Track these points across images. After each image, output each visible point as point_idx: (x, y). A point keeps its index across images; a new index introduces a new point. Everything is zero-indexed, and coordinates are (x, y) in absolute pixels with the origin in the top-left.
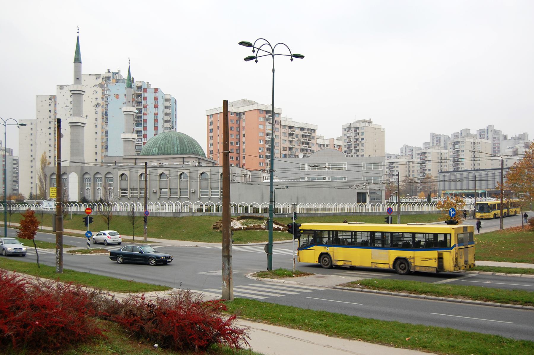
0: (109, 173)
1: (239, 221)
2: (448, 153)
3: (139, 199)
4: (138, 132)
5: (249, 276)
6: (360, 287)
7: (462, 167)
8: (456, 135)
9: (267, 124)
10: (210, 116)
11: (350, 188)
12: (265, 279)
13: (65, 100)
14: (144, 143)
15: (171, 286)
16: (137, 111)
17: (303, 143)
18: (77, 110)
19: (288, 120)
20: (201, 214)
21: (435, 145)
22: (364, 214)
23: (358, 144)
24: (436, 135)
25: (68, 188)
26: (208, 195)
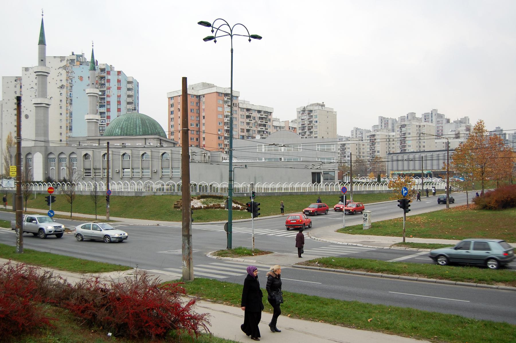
0: (73, 153)
1: (199, 201)
2: (396, 134)
3: (102, 179)
4: (101, 113)
5: (209, 255)
6: (318, 266)
7: (409, 149)
8: (402, 119)
9: (226, 106)
10: (171, 98)
11: (306, 167)
12: (225, 258)
13: (30, 82)
14: (108, 124)
15: (132, 266)
16: (100, 93)
17: (260, 125)
18: (43, 92)
19: (246, 103)
20: (163, 194)
21: (383, 127)
22: (318, 193)
23: (312, 127)
24: (384, 118)
25: (33, 168)
26: (169, 175)
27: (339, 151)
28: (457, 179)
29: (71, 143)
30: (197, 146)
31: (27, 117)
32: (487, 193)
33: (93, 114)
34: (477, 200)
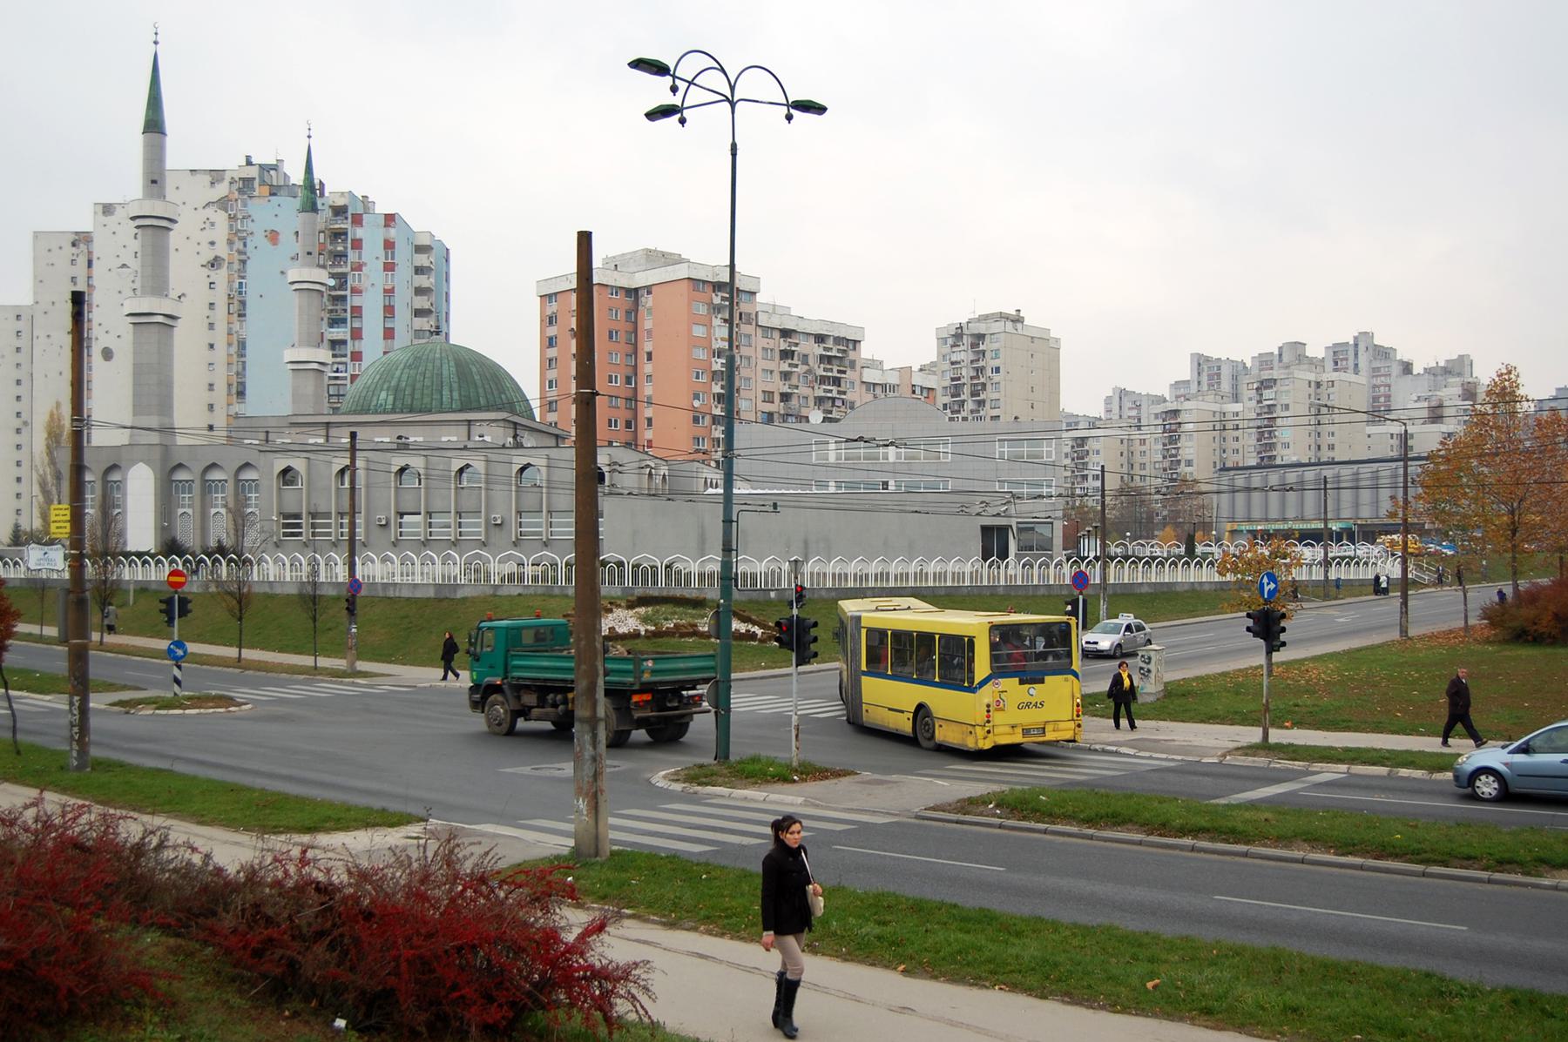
0: (247, 465)
1: (631, 613)
2: (1246, 408)
3: (335, 545)
4: (335, 344)
5: (660, 779)
6: (994, 815)
8: (1264, 361)
9: (717, 322)
10: (547, 298)
11: (963, 511)
12: (709, 789)
13: (119, 247)
14: (354, 377)
16: (332, 282)
17: (823, 380)
18: (156, 281)
20: (519, 590)
21: (1205, 388)
23: (984, 385)
24: (1208, 359)
26: (540, 534)
27: (1068, 461)
28: (1432, 547)
29: (241, 435)
30: (627, 445)
31: (107, 354)
32: (1528, 592)
33: (309, 345)
34: (1496, 616)
